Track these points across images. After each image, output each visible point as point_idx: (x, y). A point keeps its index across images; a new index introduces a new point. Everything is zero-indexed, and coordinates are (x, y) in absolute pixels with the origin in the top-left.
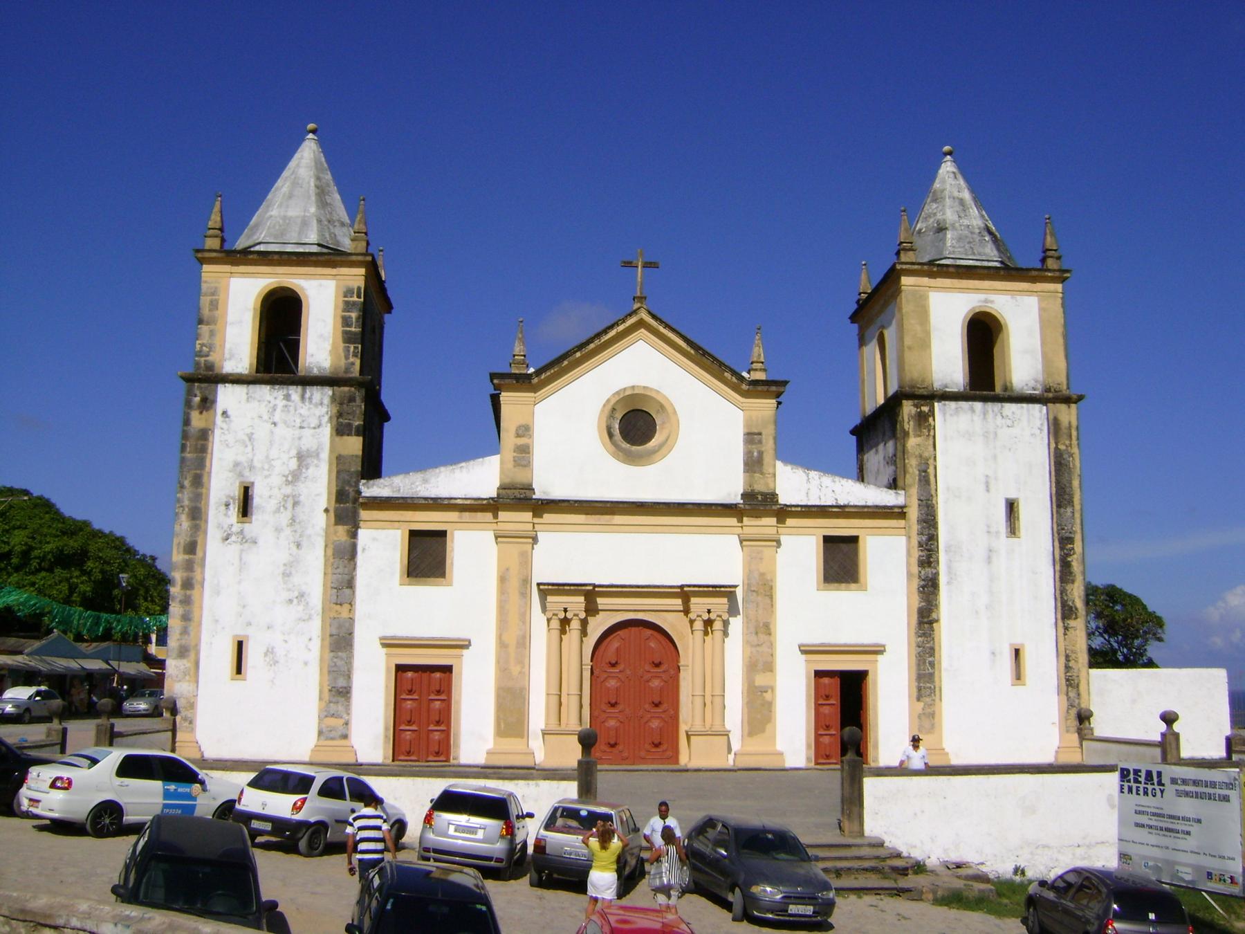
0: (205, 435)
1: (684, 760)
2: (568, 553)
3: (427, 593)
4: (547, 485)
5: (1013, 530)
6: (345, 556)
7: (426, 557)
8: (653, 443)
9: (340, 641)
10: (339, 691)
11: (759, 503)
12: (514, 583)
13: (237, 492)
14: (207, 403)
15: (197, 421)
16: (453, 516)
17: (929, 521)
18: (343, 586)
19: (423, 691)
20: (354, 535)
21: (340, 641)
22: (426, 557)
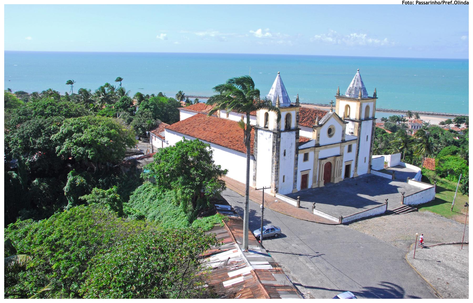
0: (279, 142)
1: (332, 181)
2: (323, 153)
3: (306, 163)
4: (321, 143)
5: (367, 140)
6: (297, 159)
7: (306, 158)
8: (331, 133)
9: (296, 173)
10: (295, 181)
11: (343, 141)
12: (317, 160)
13: (283, 152)
14: (280, 137)
15: (278, 141)
16: (309, 149)
17: (359, 141)
18: (296, 165)
19: (305, 178)
20: (298, 156)
21: (296, 173)
22: (306, 158)
